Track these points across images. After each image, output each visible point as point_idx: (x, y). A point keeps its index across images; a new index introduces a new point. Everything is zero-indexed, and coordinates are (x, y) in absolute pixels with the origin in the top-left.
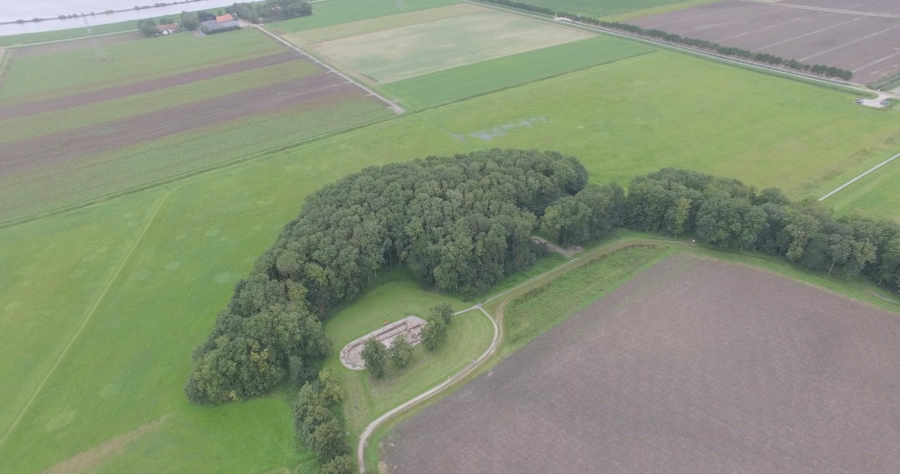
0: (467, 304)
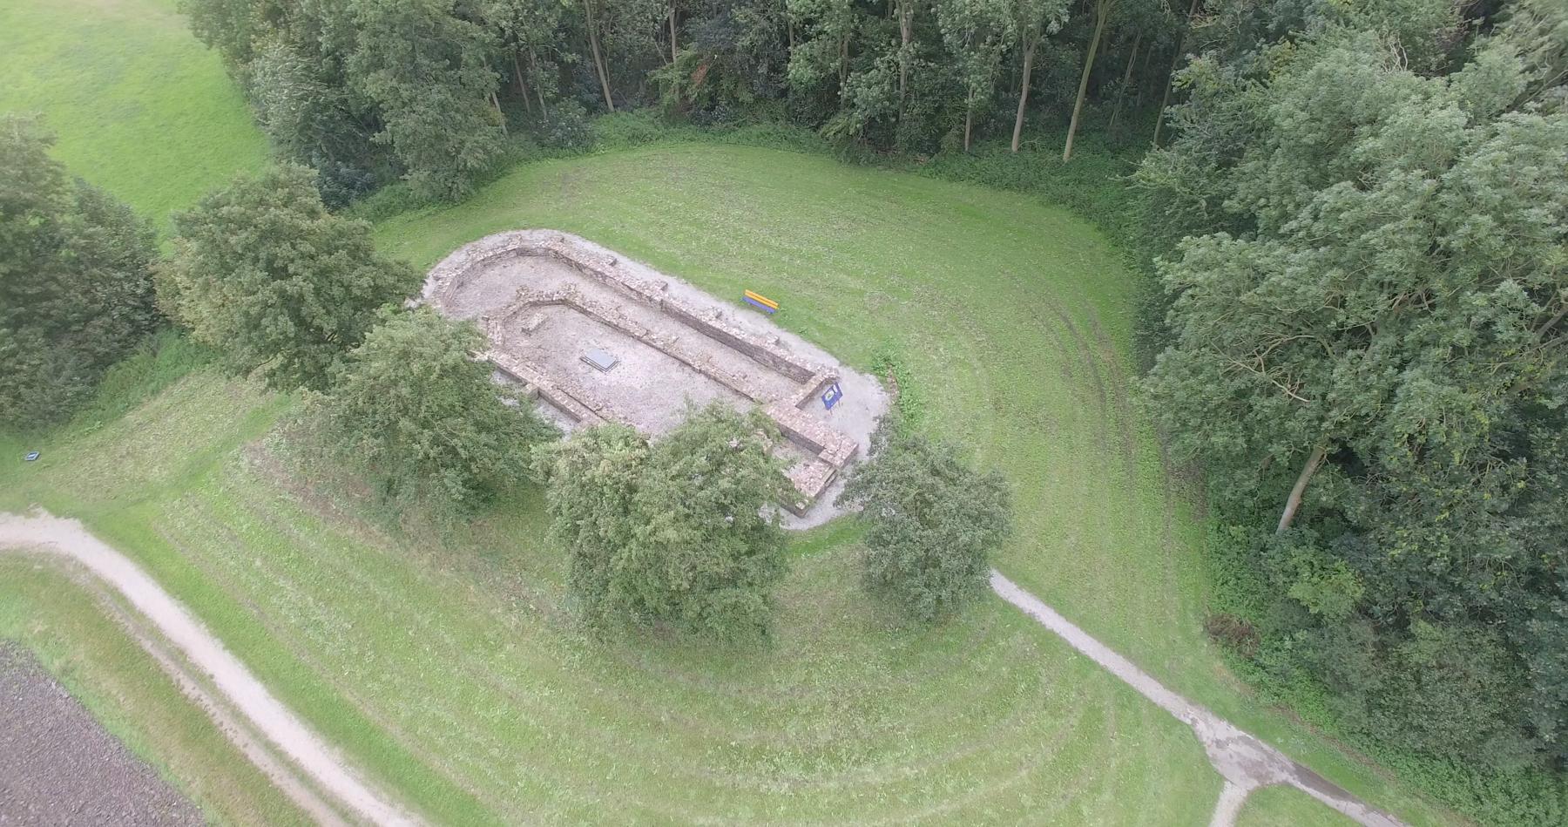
0: (1215, 664)
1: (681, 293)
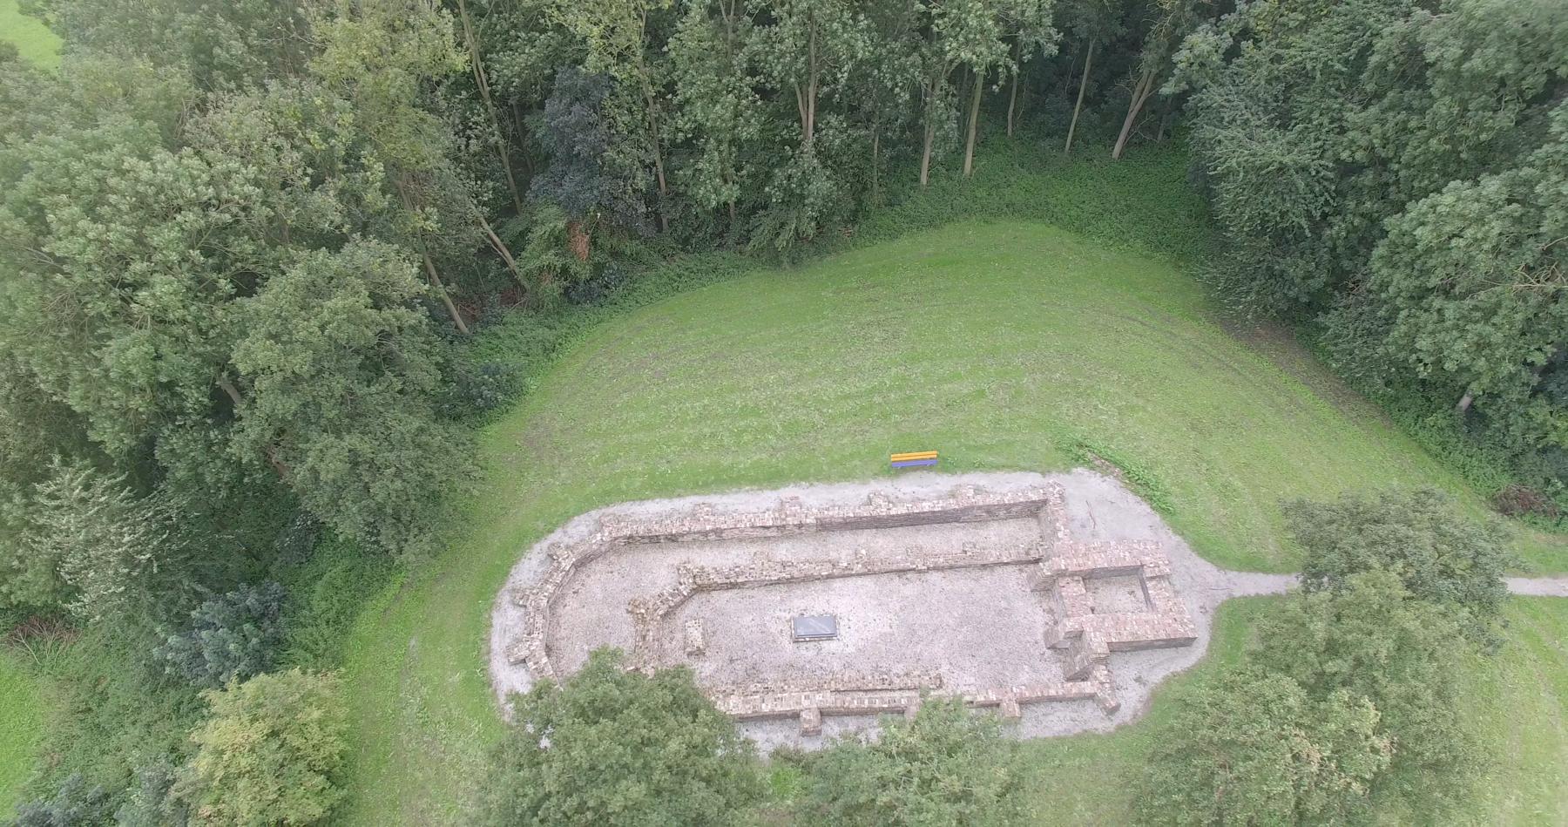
1: (815, 500)
